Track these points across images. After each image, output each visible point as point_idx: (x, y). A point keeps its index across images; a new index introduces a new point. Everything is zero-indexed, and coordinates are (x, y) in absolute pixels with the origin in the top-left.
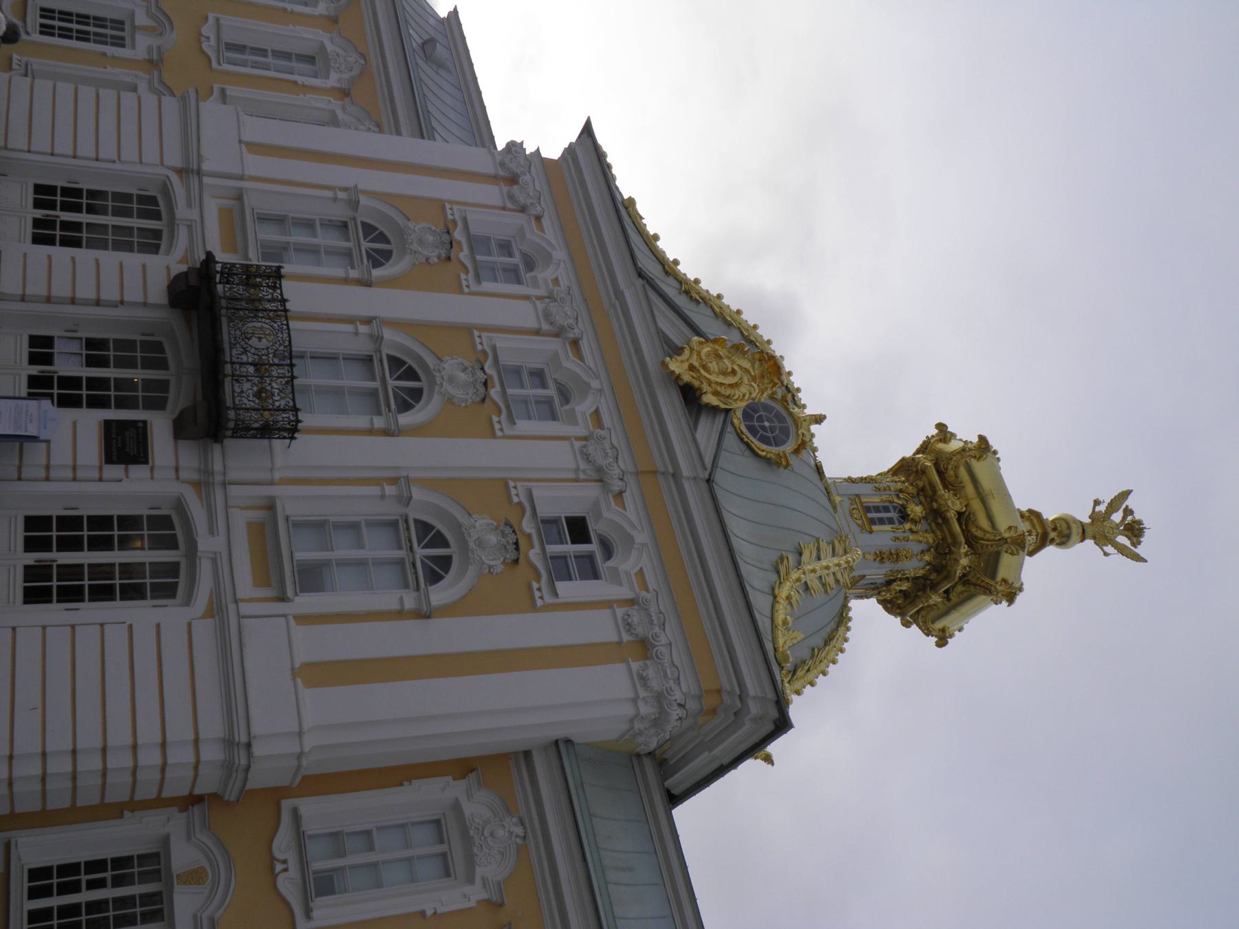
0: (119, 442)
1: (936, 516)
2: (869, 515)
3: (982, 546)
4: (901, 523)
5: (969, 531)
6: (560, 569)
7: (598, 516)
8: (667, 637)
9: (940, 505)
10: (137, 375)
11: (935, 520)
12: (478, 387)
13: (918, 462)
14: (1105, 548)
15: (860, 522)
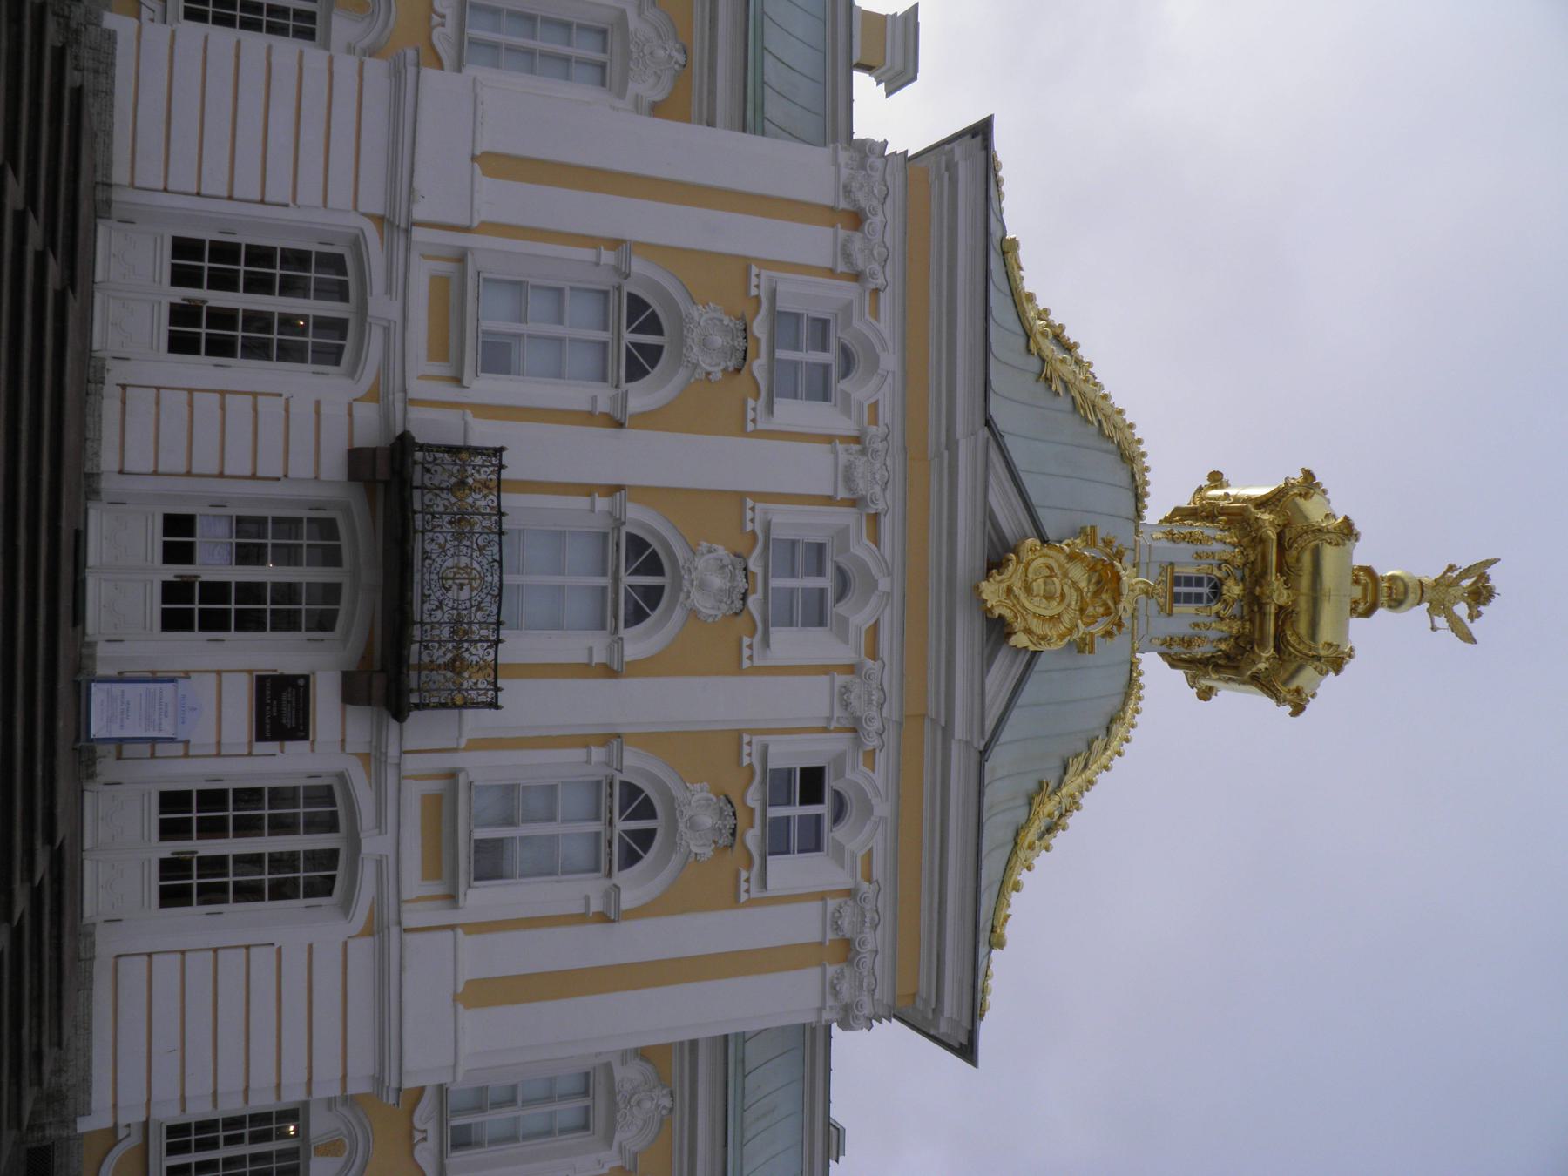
0: (275, 710)
1: (1254, 602)
2: (1177, 589)
3: (1290, 654)
4: (1209, 601)
5: (1283, 631)
6: (778, 840)
7: (840, 774)
8: (875, 942)
9: (1263, 593)
10: (303, 574)
11: (1250, 604)
12: (734, 598)
13: (1261, 527)
14: (1436, 618)
15: (1162, 601)
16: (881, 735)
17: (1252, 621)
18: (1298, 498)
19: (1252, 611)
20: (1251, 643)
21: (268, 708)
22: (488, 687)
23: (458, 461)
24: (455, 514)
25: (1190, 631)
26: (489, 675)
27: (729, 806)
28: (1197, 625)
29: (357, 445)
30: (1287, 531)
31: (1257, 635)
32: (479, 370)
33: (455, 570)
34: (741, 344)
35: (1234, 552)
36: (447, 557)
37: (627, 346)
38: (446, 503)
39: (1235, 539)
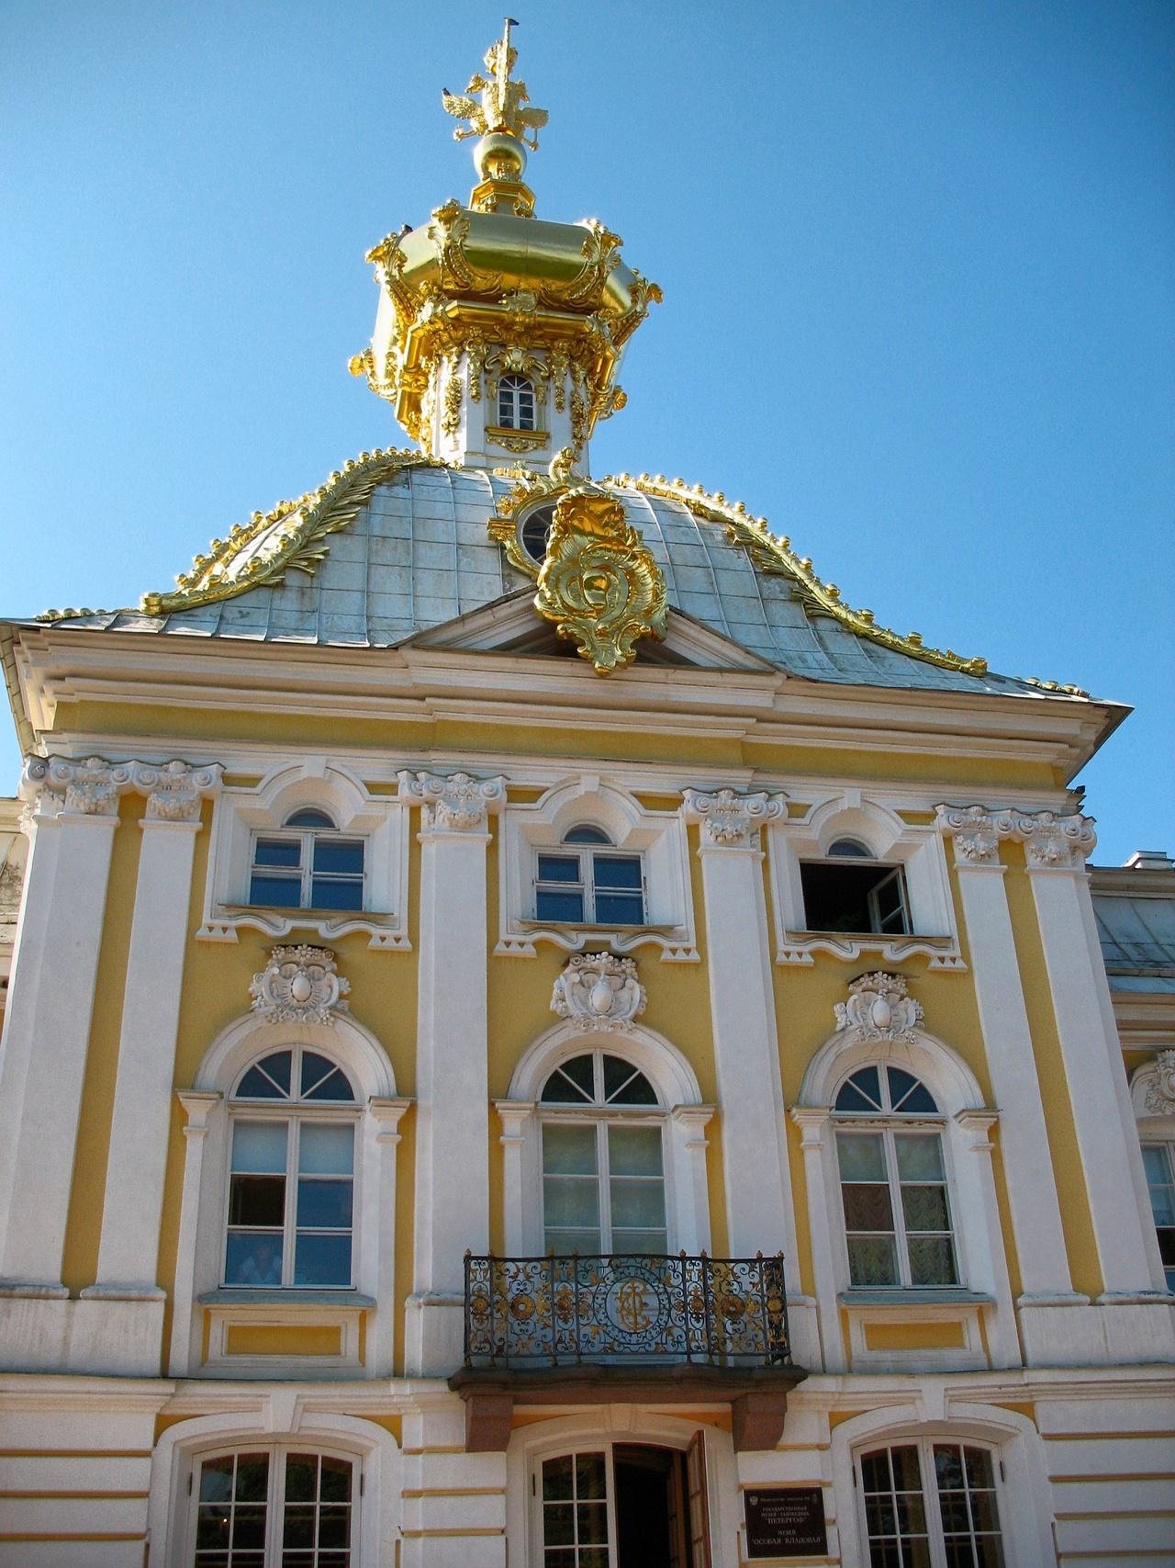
0: (788, 1533)
2: (517, 425)
4: (528, 387)
12: (620, 969)
16: (770, 795)
17: (555, 338)
18: (403, 269)
19: (541, 336)
20: (579, 341)
21: (787, 1541)
22: (758, 1270)
23: (488, 1312)
24: (554, 1314)
25: (567, 413)
26: (744, 1269)
27: (862, 979)
28: (560, 406)
29: (462, 1440)
30: (445, 287)
31: (570, 333)
32: (347, 1287)
33: (624, 1313)
34: (304, 952)
35: (469, 352)
36: (609, 1324)
37: (306, 1098)
38: (540, 1326)
39: (454, 350)
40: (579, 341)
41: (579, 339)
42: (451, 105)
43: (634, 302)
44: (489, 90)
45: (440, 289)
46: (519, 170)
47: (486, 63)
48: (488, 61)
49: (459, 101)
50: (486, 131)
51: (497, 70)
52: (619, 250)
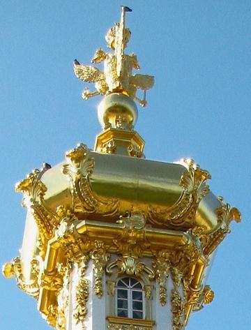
2: (130, 315)
4: (139, 286)
5: (168, 222)
17: (159, 249)
18: (44, 196)
19: (149, 248)
20: (178, 252)
25: (169, 306)
28: (163, 301)
30: (76, 210)
35: (94, 260)
39: (83, 258)
40: (178, 252)
41: (178, 250)
42: (80, 72)
43: (220, 221)
44: (109, 61)
45: (72, 211)
46: (132, 121)
47: (107, 41)
48: (108, 38)
49: (86, 69)
50: (107, 92)
51: (115, 46)
52: (208, 182)
